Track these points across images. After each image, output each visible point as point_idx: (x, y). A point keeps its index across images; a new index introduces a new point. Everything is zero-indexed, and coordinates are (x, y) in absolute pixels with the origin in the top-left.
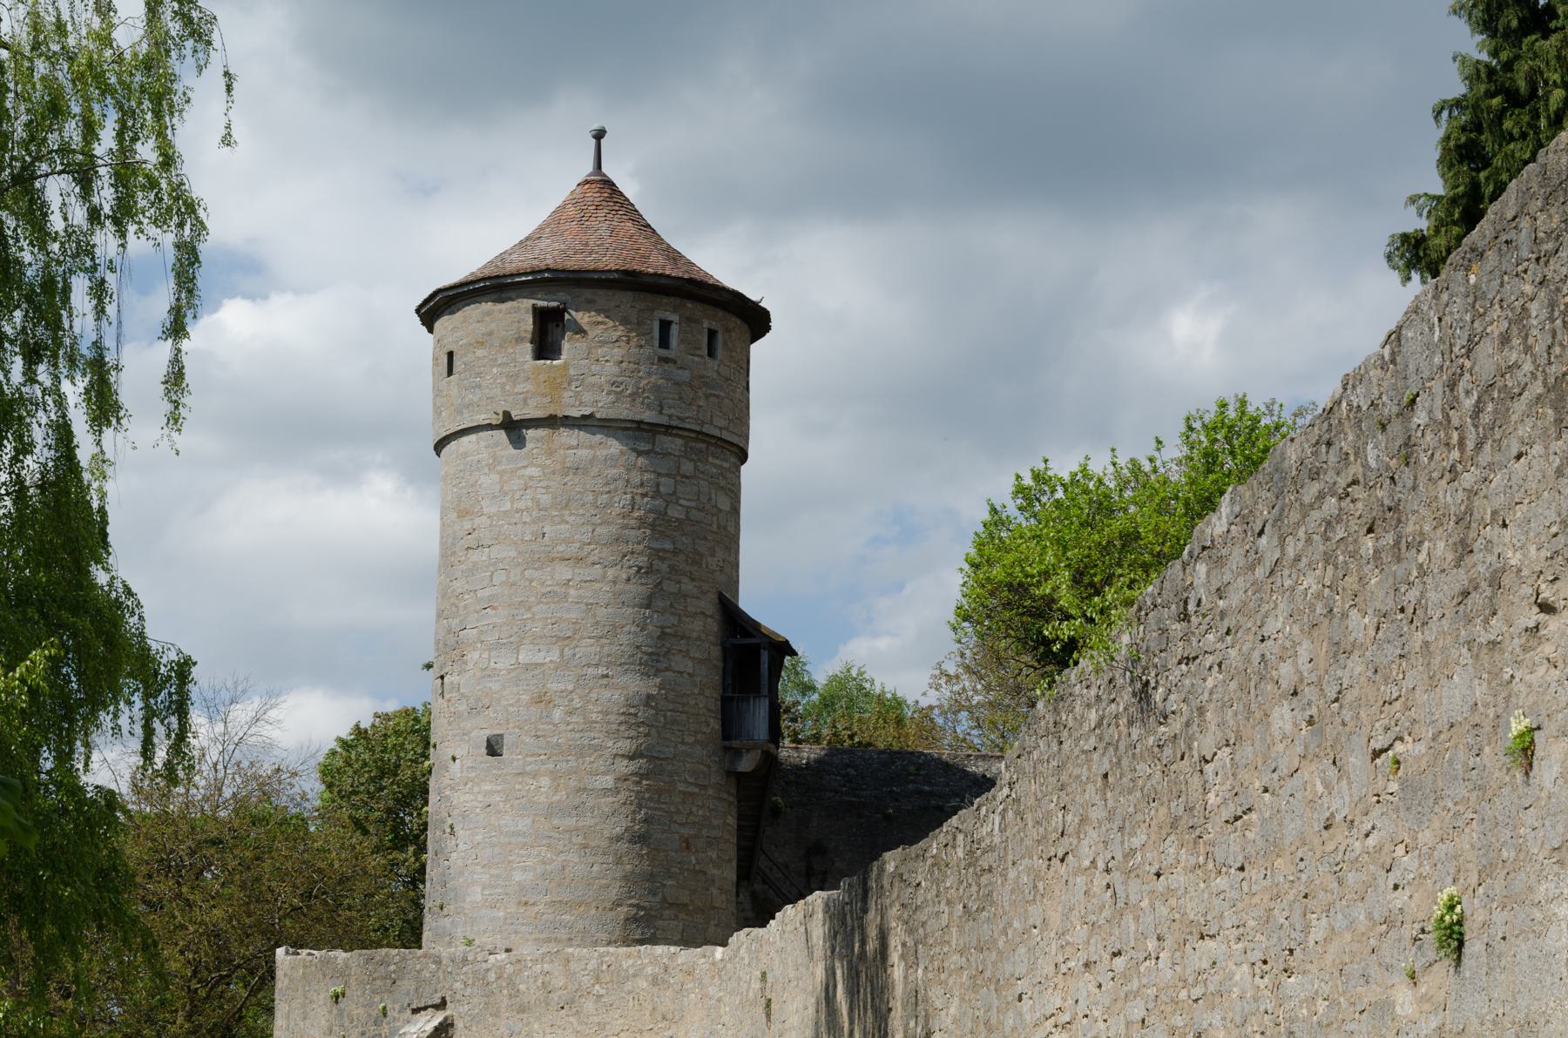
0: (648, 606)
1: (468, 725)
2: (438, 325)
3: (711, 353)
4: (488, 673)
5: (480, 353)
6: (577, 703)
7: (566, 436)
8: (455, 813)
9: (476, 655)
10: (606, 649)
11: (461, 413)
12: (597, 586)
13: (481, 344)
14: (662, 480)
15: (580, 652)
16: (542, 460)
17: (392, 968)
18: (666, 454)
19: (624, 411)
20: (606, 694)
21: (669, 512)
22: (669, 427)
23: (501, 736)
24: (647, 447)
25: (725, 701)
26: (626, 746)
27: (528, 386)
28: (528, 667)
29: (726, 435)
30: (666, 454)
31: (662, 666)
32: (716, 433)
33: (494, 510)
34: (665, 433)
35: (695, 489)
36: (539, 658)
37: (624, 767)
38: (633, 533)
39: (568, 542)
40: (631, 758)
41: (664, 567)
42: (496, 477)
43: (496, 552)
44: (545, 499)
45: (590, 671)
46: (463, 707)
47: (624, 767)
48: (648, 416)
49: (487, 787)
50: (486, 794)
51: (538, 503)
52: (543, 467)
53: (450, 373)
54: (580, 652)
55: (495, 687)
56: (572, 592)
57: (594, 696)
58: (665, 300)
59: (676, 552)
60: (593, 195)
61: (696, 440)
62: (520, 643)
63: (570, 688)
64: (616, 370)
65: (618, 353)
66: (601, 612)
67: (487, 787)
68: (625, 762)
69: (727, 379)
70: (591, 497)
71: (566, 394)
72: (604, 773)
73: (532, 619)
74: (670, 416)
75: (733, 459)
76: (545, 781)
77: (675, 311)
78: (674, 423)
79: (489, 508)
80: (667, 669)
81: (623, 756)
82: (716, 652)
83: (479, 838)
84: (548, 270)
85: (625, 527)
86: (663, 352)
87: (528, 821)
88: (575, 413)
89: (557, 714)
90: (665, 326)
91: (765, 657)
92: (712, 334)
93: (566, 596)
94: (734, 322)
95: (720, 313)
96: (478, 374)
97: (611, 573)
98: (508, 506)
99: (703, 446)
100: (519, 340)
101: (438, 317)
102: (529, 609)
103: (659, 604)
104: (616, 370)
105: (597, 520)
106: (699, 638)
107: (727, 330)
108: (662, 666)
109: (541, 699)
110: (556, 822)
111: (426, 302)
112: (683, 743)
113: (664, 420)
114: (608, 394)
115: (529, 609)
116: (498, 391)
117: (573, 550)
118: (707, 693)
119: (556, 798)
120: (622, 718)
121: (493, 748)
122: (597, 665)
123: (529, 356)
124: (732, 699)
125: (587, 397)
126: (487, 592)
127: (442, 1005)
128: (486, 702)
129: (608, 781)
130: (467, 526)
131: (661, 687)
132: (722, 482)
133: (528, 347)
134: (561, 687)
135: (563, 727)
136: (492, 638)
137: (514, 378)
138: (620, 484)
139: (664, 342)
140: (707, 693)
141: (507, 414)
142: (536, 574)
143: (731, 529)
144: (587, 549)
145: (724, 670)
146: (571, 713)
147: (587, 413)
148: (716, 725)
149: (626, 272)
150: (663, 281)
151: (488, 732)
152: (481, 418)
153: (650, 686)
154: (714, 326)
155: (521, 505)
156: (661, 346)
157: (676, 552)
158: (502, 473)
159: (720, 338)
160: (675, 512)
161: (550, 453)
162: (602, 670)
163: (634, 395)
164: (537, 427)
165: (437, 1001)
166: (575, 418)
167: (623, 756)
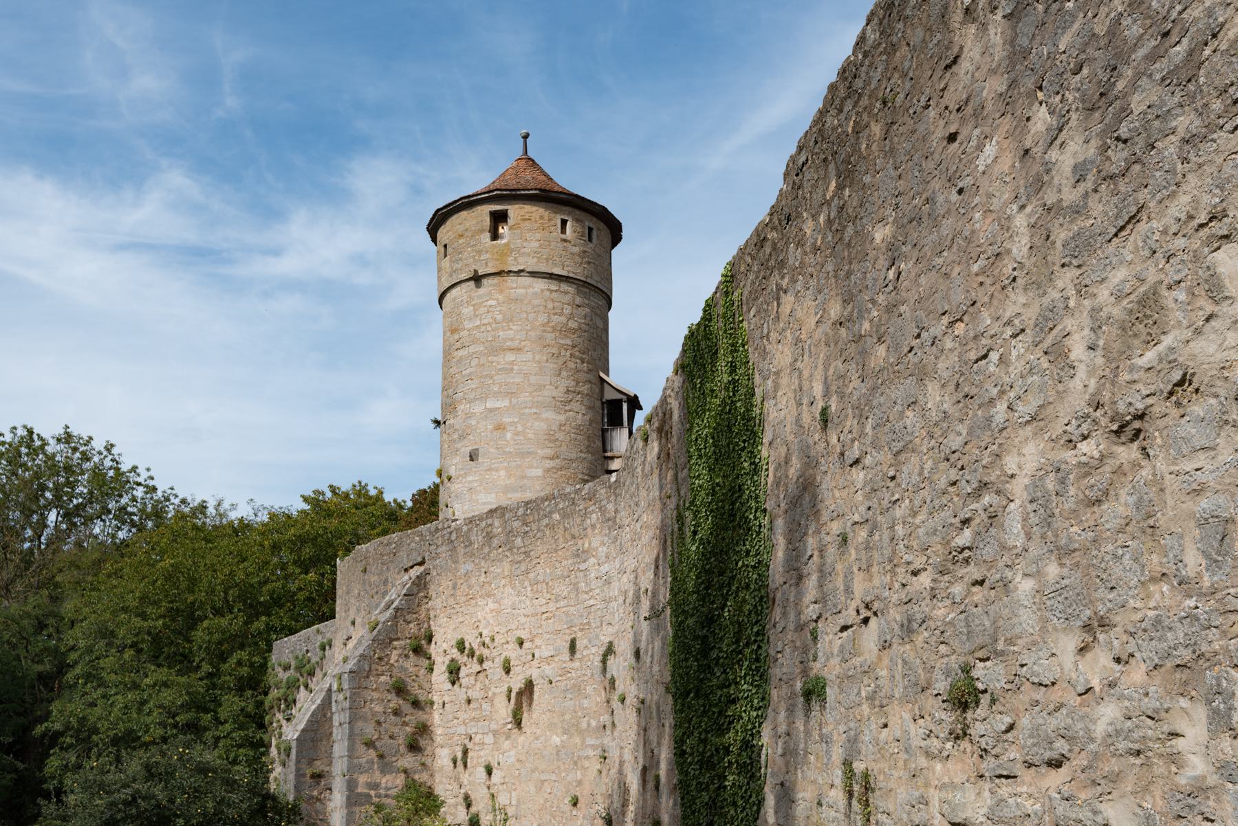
0: (559, 375)
1: (459, 445)
2: (439, 235)
3: (590, 240)
4: (469, 416)
5: (461, 241)
6: (520, 428)
7: (512, 281)
8: (453, 495)
9: (462, 407)
10: (536, 399)
11: (451, 276)
12: (529, 364)
13: (461, 236)
14: (565, 306)
15: (521, 399)
16: (496, 296)
17: (394, 545)
18: (566, 293)
19: (543, 268)
20: (537, 424)
21: (570, 325)
22: (567, 277)
23: (477, 449)
24: (557, 288)
25: (604, 431)
26: (550, 452)
27: (488, 256)
28: (491, 410)
29: (599, 286)
30: (566, 293)
31: (567, 408)
32: (595, 284)
33: (471, 326)
34: (566, 281)
35: (583, 313)
36: (498, 404)
37: (549, 464)
38: (549, 335)
39: (512, 340)
40: (552, 459)
41: (568, 353)
42: (472, 308)
43: (472, 349)
44: (499, 317)
45: (527, 411)
46: (456, 436)
47: (549, 464)
48: (557, 271)
49: (470, 478)
50: (470, 482)
51: (495, 320)
52: (497, 300)
53: (446, 256)
54: (521, 399)
55: (473, 422)
56: (515, 367)
57: (529, 424)
58: (564, 208)
59: (573, 347)
60: (523, 164)
61: (583, 286)
62: (486, 398)
63: (516, 420)
64: (537, 244)
65: (538, 236)
66: (533, 379)
67: (470, 478)
68: (548, 461)
69: (599, 256)
70: (524, 315)
71: (509, 259)
72: (536, 468)
73: (493, 383)
74: (568, 271)
75: (604, 302)
76: (502, 473)
77: (569, 214)
78: (571, 275)
79: (468, 325)
80: (570, 411)
81: (547, 458)
82: (598, 404)
83: (466, 507)
84: (497, 190)
85: (544, 331)
86: (563, 236)
87: (493, 496)
88: (516, 270)
89: (509, 435)
90: (564, 222)
91: (625, 406)
92: (590, 229)
93: (512, 369)
94: (602, 226)
95: (595, 219)
96: (460, 253)
97: (537, 357)
98: (478, 323)
99: (587, 290)
100: (482, 231)
101: (438, 229)
102: (492, 378)
103: (564, 374)
104: (537, 244)
105: (529, 328)
106: (587, 395)
107: (598, 229)
108: (567, 408)
109: (500, 427)
110: (509, 495)
111: (432, 220)
112: (581, 451)
113: (564, 273)
114: (533, 257)
115: (492, 378)
116: (471, 260)
117: (516, 344)
118: (594, 425)
119: (509, 482)
120: (546, 437)
121: (472, 457)
122: (530, 408)
123: (488, 239)
124: (607, 430)
125: (521, 260)
126: (468, 371)
127: (421, 564)
128: (469, 431)
129: (539, 472)
130: (456, 337)
131: (567, 419)
132: (599, 312)
133: (488, 235)
134: (511, 420)
135: (512, 442)
136: (471, 396)
137: (480, 252)
138: (541, 308)
139: (563, 230)
140: (594, 425)
141: (476, 271)
142: (495, 359)
143: (604, 338)
144: (523, 343)
145: (603, 414)
146: (517, 434)
147: (521, 268)
148: (600, 444)
149: (540, 190)
150: (562, 196)
151: (470, 448)
152: (463, 276)
153: (562, 418)
154: (591, 225)
155: (486, 321)
156: (562, 233)
157: (573, 347)
158: (474, 305)
159: (595, 233)
160: (572, 324)
161: (501, 292)
162: (534, 410)
163: (547, 260)
164: (491, 278)
165: (419, 559)
166: (515, 272)
167: (547, 458)
